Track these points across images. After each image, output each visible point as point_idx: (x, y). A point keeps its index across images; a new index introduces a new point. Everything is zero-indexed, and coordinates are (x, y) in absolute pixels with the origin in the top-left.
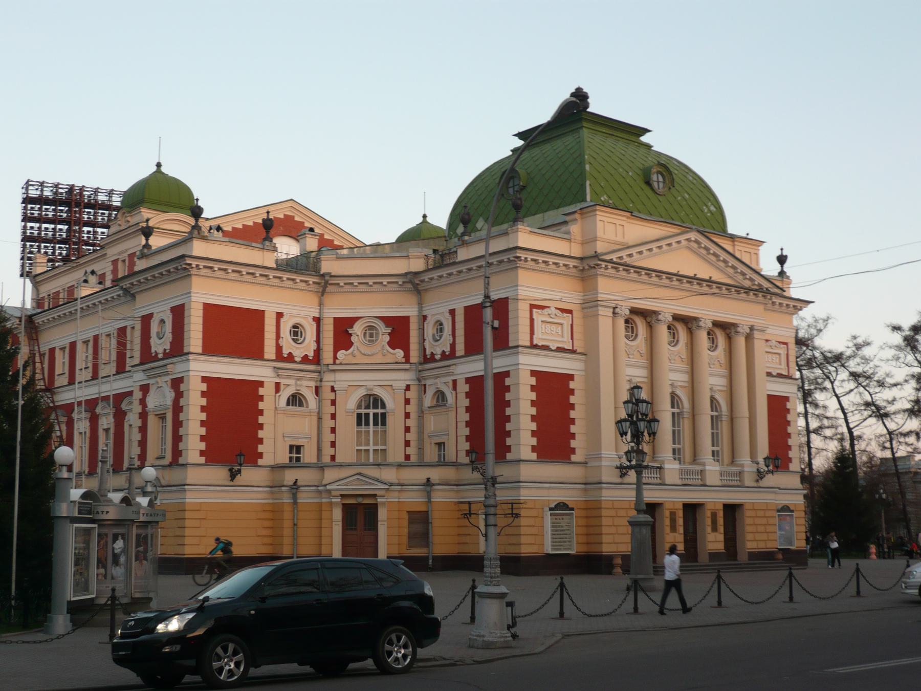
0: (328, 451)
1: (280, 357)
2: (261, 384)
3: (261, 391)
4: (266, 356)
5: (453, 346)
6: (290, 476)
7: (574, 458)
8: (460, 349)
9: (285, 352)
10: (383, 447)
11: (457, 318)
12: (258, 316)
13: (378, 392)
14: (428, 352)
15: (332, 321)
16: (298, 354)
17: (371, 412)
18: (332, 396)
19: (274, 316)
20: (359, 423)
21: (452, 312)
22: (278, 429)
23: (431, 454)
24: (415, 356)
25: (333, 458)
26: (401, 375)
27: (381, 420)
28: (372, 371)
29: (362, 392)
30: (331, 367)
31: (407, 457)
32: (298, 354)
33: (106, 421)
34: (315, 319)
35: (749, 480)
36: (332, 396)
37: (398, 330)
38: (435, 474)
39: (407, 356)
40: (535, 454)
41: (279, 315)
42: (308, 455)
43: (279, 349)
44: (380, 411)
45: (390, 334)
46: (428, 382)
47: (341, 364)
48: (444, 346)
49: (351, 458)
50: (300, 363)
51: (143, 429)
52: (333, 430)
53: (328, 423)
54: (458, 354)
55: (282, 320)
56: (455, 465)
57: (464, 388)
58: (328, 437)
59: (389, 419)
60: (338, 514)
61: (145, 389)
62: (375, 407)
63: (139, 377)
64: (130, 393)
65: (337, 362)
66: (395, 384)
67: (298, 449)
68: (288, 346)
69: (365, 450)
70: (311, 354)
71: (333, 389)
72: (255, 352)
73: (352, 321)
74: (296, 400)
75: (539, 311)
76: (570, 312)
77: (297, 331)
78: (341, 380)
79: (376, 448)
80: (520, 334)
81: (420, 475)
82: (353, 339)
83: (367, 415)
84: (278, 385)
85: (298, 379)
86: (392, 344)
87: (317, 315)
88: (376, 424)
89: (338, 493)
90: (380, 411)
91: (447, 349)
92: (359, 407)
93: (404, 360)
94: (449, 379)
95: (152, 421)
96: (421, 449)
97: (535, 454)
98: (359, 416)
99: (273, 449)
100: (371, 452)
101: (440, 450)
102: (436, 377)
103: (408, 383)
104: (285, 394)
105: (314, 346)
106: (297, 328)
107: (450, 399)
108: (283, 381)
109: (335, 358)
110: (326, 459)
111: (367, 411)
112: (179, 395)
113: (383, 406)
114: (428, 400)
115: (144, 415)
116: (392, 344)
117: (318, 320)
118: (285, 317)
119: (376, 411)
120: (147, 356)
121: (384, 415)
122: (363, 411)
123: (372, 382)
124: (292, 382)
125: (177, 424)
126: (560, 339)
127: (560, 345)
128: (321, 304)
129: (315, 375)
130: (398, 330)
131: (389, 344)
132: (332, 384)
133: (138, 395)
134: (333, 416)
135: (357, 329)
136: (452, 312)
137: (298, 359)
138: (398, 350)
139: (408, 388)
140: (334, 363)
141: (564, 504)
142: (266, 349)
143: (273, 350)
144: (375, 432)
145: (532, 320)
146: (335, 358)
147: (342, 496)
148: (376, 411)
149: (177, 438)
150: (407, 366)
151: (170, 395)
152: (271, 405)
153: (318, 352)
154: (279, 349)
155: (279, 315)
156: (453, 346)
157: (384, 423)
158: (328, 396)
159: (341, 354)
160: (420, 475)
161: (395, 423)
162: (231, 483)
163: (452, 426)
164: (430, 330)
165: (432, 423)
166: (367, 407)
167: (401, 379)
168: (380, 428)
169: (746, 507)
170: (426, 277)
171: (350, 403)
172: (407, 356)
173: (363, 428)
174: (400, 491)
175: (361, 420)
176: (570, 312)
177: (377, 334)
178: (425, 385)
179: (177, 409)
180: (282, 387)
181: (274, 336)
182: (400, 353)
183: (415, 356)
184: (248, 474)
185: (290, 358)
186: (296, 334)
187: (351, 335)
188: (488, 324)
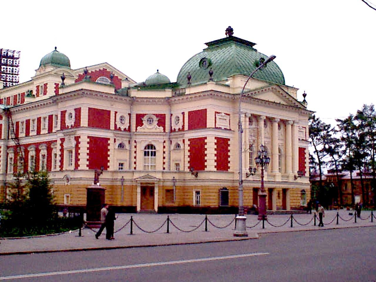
5: (183, 126)
8: (186, 128)
9: (118, 127)
10: (154, 164)
11: (185, 116)
12: (109, 112)
13: (153, 143)
17: (150, 150)
20: (145, 155)
21: (183, 113)
23: (173, 168)
24: (168, 130)
25: (135, 168)
26: (162, 137)
31: (164, 169)
37: (161, 120)
38: (177, 176)
39: (164, 129)
41: (116, 113)
43: (116, 125)
44: (153, 150)
49: (142, 169)
56: (184, 172)
57: (187, 143)
60: (139, 190)
62: (152, 149)
65: (137, 131)
71: (135, 142)
72: (107, 127)
74: (121, 146)
83: (148, 152)
84: (115, 139)
85: (122, 137)
86: (159, 125)
88: (152, 155)
90: (153, 150)
91: (181, 127)
92: (145, 148)
98: (145, 152)
104: (118, 143)
107: (182, 147)
109: (136, 129)
113: (155, 149)
114: (172, 147)
116: (159, 125)
119: (152, 150)
121: (155, 152)
122: (147, 150)
123: (150, 140)
136: (183, 113)
139: (164, 142)
146: (136, 129)
148: (152, 150)
152: (112, 147)
154: (116, 125)
155: (116, 113)
156: (183, 126)
157: (155, 155)
159: (139, 128)
163: (183, 157)
165: (174, 156)
166: (149, 148)
167: (161, 139)
171: (141, 147)
172: (164, 129)
175: (146, 154)
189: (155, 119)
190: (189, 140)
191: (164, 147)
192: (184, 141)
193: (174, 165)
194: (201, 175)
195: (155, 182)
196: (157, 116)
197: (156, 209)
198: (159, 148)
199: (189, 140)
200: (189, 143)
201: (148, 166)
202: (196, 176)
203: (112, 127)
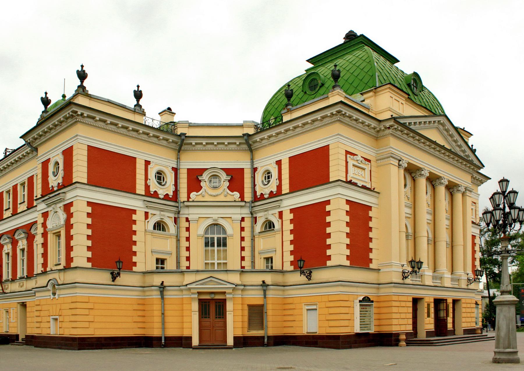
0: (184, 264)
1: (148, 193)
2: (134, 212)
3: (134, 217)
4: (138, 192)
5: (279, 187)
6: (157, 280)
7: (372, 266)
8: (286, 188)
9: (152, 190)
11: (283, 167)
13: (221, 222)
14: (258, 194)
15: (186, 171)
16: (162, 192)
18: (187, 225)
19: (144, 163)
20: (207, 244)
21: (279, 163)
22: (146, 246)
24: (248, 196)
25: (188, 268)
26: (238, 210)
27: (223, 243)
28: (214, 208)
29: (210, 222)
30: (186, 204)
32: (162, 192)
33: (22, 244)
34: (173, 168)
35: (463, 285)
36: (187, 225)
37: (235, 179)
38: (269, 278)
40: (349, 262)
42: (170, 265)
43: (147, 187)
45: (229, 181)
46: (258, 215)
47: (193, 201)
48: (273, 187)
50: (163, 199)
51: (45, 245)
52: (188, 249)
53: (184, 244)
54: (283, 193)
55: (149, 166)
56: (282, 272)
57: (288, 216)
58: (184, 254)
59: (228, 242)
61: (45, 215)
63: (42, 207)
64: (36, 222)
66: (233, 217)
67: (161, 261)
68: (154, 186)
69: (211, 263)
70: (171, 194)
71: (187, 220)
74: (159, 226)
75: (352, 157)
76: (369, 161)
77: (160, 176)
78: (193, 213)
79: (219, 262)
80: (336, 172)
81: (257, 279)
82: (202, 184)
84: (146, 214)
85: (162, 210)
86: (231, 188)
87: (175, 166)
88: (219, 245)
89: (196, 291)
90: (222, 236)
91: (274, 190)
93: (240, 199)
94: (277, 211)
95: (50, 237)
96: (253, 262)
97: (349, 262)
99: (143, 260)
100: (216, 265)
101: (267, 262)
102: (266, 210)
103: (243, 216)
104: (153, 221)
105: (173, 188)
106: (161, 174)
107: (277, 226)
108: (150, 211)
109: (189, 197)
110: (184, 269)
111: (212, 236)
112: (70, 216)
113: (225, 232)
114: (258, 227)
115: (45, 235)
116: (231, 188)
117: (176, 170)
118: (151, 164)
120: (47, 191)
121: (225, 239)
122: (210, 236)
123: (215, 214)
124: (157, 212)
125: (69, 238)
126: (363, 179)
127: (365, 184)
128: (178, 159)
129: (174, 209)
130: (235, 179)
131: (228, 187)
132: (187, 216)
133: (41, 220)
134: (188, 239)
135: (205, 176)
136: (279, 163)
137: (161, 197)
138: (235, 193)
139: (243, 219)
140: (188, 201)
141: (368, 297)
142: (138, 186)
143: (143, 188)
145: (347, 163)
146: (189, 197)
147: (199, 293)
148: (219, 236)
149: (69, 249)
150: (243, 204)
151: (63, 216)
152: (142, 227)
153: (176, 192)
154: (147, 187)
155: (147, 163)
156: (279, 187)
157: (225, 245)
160: (257, 279)
161: (233, 244)
162: (113, 283)
163: (279, 245)
164: (259, 177)
165: (262, 244)
167: (237, 213)
168: (222, 248)
169: (463, 301)
170: (258, 138)
171: (199, 230)
173: (210, 248)
174: (242, 290)
176: (369, 161)
177: (220, 181)
178: (256, 218)
179: (69, 226)
180: (150, 216)
181: (143, 177)
182: (237, 195)
183: (248, 196)
184: (125, 278)
185: (155, 195)
186: (159, 178)
187: (200, 181)
188: (310, 169)
189: (224, 176)
190: (292, 211)
191: (242, 229)
192: (281, 214)
194: (319, 275)
195: (227, 291)
197: (230, 342)
198: (232, 230)
199: (292, 211)
201: (214, 263)
202: (309, 277)
203: (140, 188)
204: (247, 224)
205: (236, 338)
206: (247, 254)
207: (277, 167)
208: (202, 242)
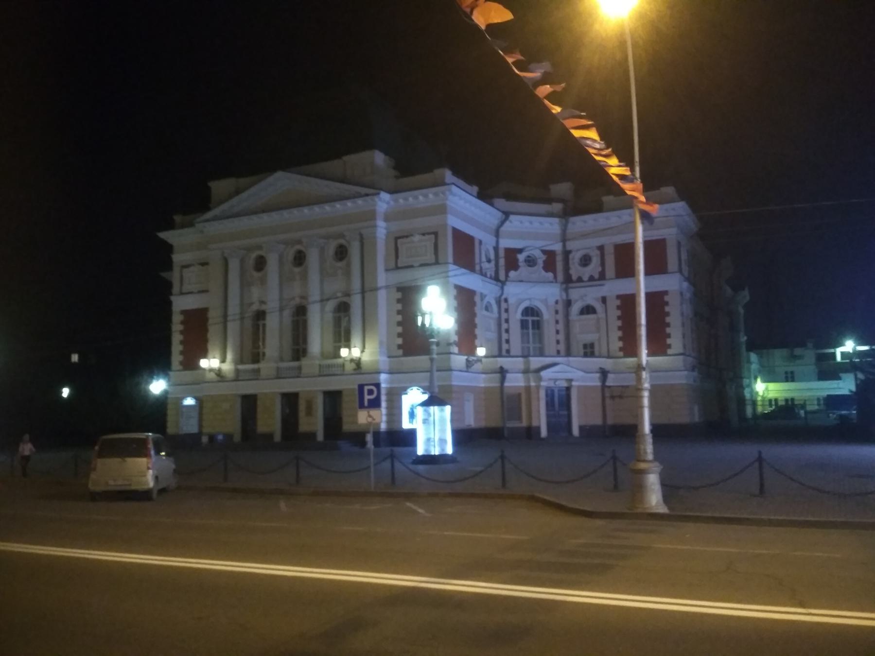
14: (574, 278)
17: (530, 319)
27: (537, 325)
31: (558, 352)
39: (555, 277)
44: (535, 318)
62: (533, 315)
73: (520, 251)
88: (533, 328)
90: (535, 318)
92: (522, 315)
109: (507, 276)
139: (557, 302)
144: (534, 334)
146: (507, 276)
158: (504, 305)
159: (512, 274)
172: (555, 277)
175: (524, 325)
182: (550, 275)
189: (541, 258)
193: (581, 347)
196: (544, 252)
199: (619, 297)
200: (618, 302)
204: (560, 307)
205: (582, 428)
206: (561, 337)
207: (598, 252)
208: (519, 325)
